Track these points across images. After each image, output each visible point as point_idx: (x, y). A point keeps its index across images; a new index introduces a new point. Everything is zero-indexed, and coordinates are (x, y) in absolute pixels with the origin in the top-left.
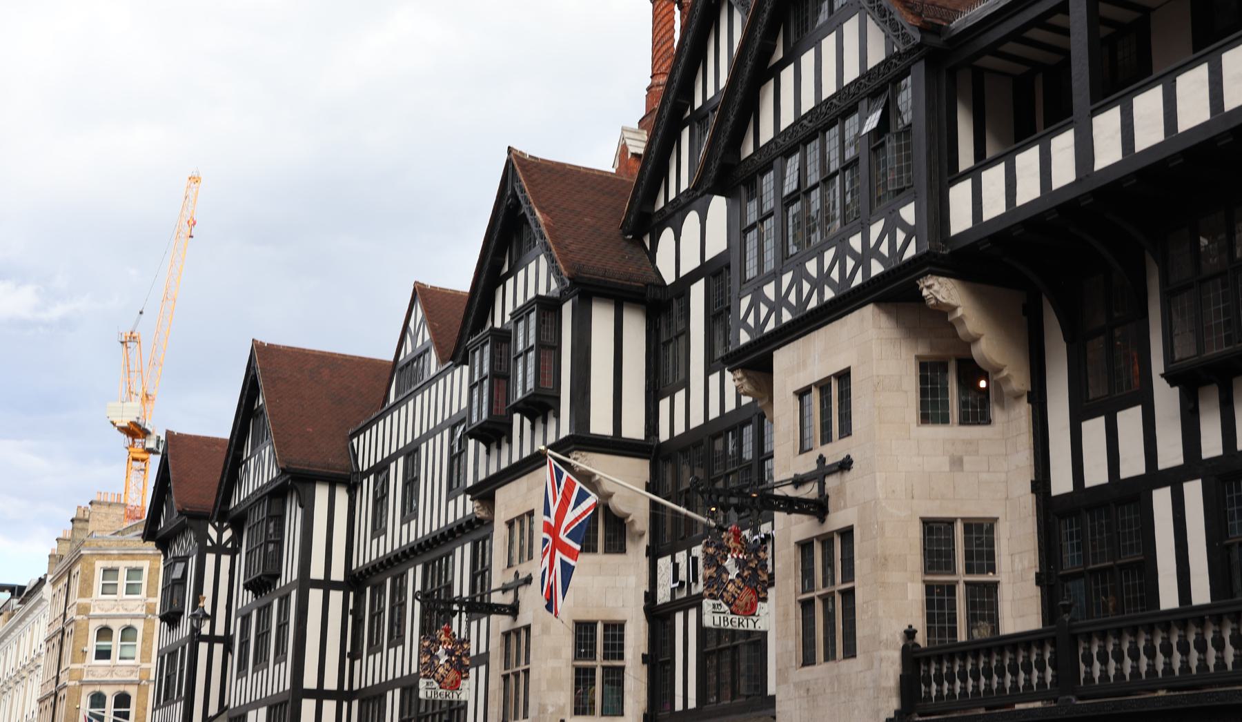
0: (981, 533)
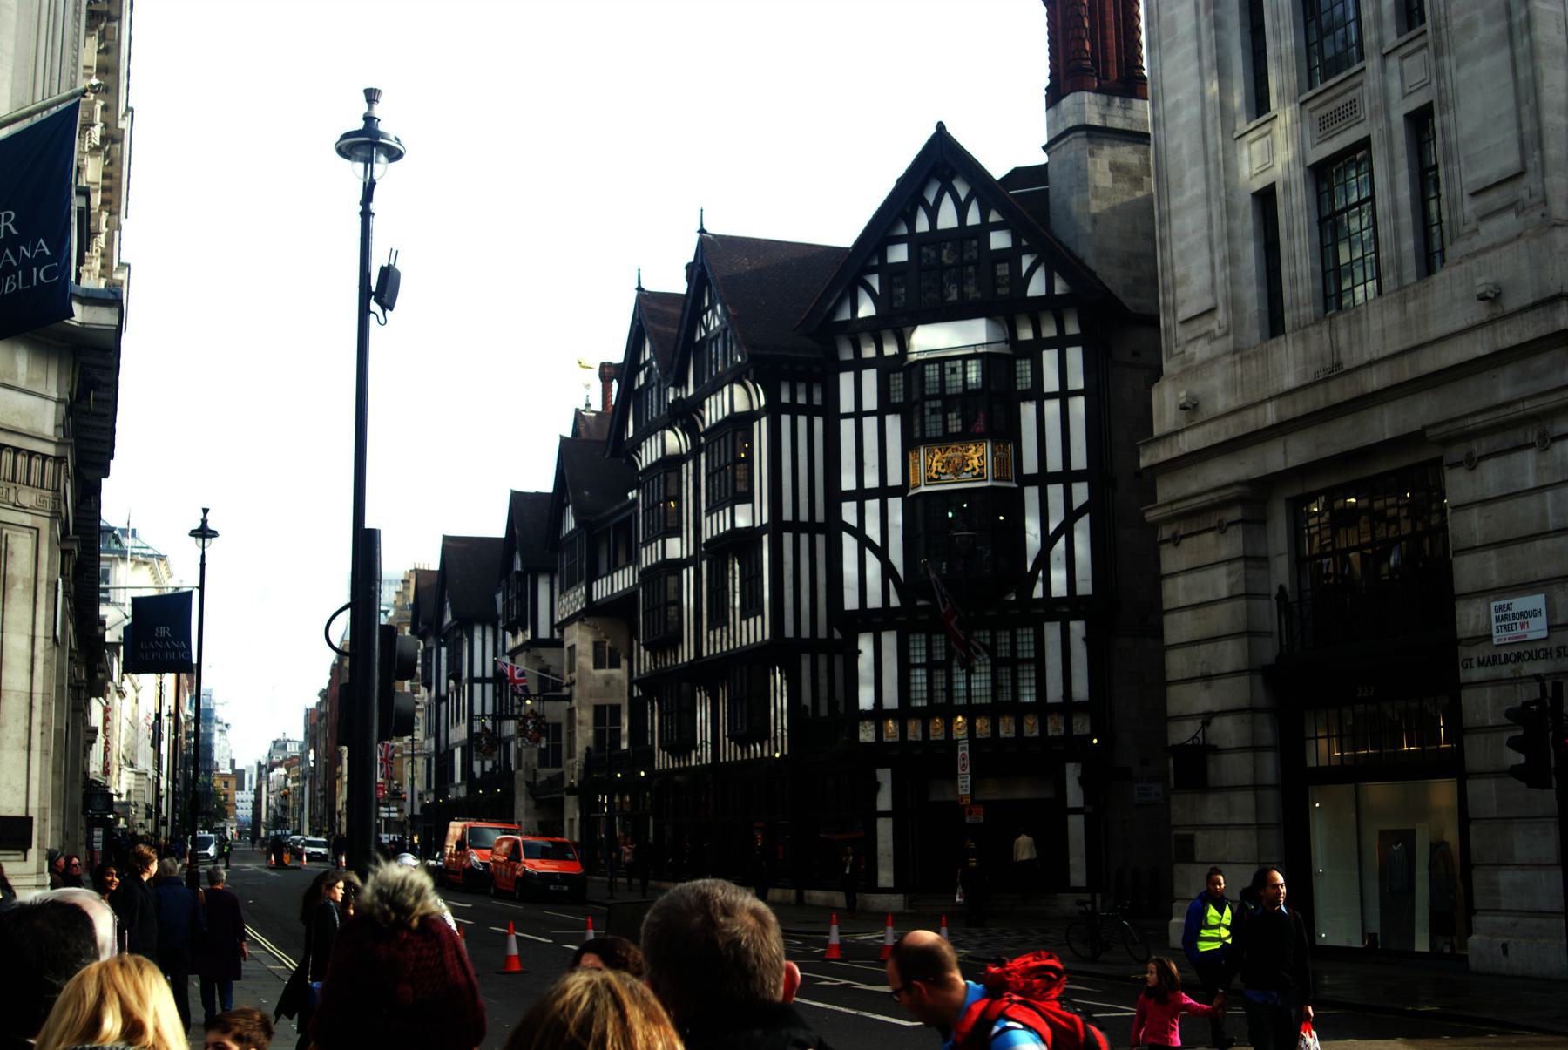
0: (616, 710)
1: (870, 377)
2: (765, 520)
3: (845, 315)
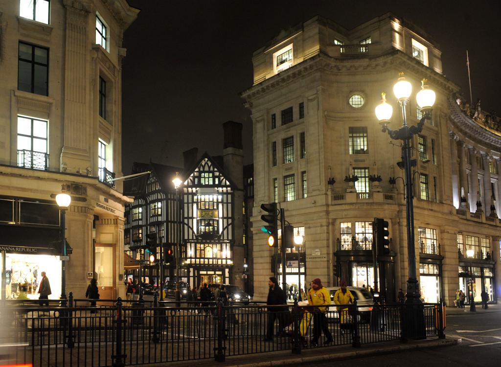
2: (165, 220)
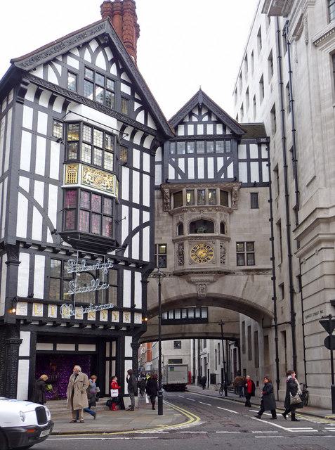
1: (43, 118)
3: (39, 74)
